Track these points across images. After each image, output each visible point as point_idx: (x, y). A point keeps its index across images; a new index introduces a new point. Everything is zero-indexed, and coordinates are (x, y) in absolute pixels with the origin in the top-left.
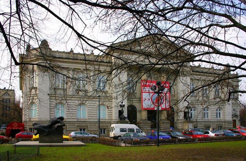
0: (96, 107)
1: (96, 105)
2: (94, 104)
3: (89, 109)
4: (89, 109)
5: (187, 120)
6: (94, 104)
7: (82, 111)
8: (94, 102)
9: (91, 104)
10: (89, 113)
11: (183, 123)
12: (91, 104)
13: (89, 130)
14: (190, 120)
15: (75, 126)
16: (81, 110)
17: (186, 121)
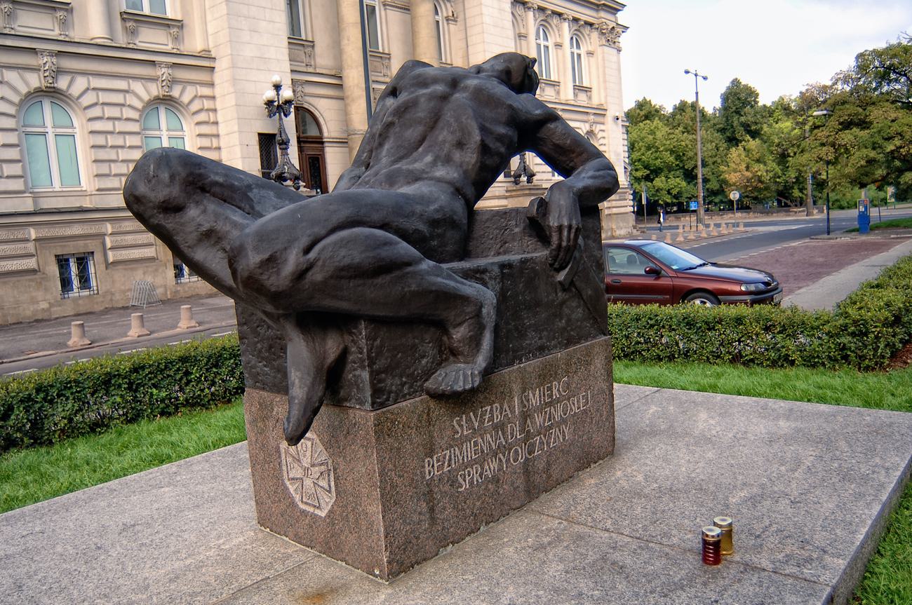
0: (135, 115)
1: (132, 100)
2: (118, 98)
3: (98, 126)
4: (98, 126)
5: (516, 183)
6: (118, 98)
7: (51, 137)
8: (122, 84)
9: (104, 97)
10: (103, 154)
11: (506, 198)
12: (104, 97)
13: (115, 263)
14: (529, 181)
15: (27, 240)
16: (44, 134)
17: (512, 187)
